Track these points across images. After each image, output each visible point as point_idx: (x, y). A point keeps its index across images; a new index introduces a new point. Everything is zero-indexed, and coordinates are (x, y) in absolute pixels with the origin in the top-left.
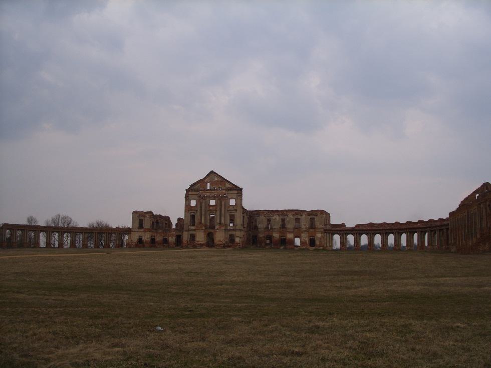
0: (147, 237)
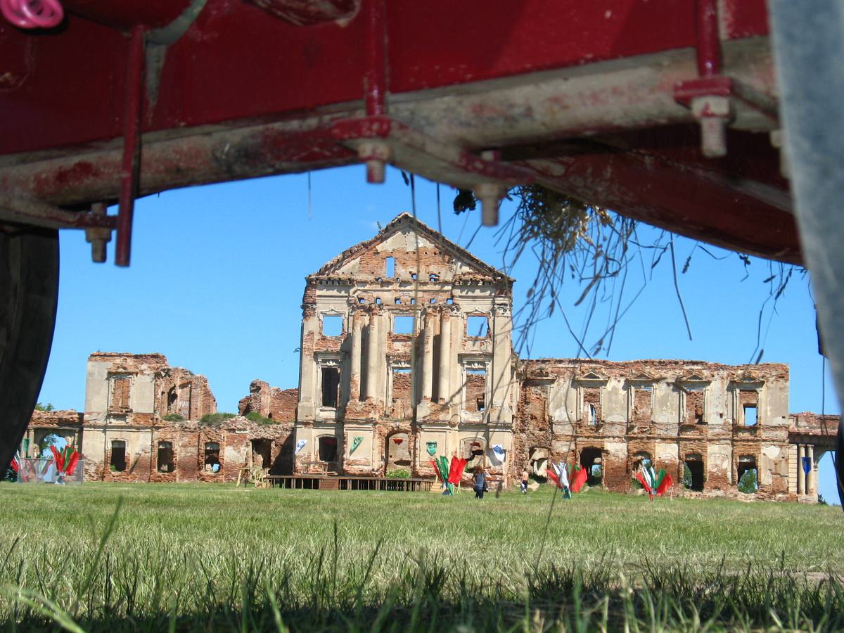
0: (139, 445)
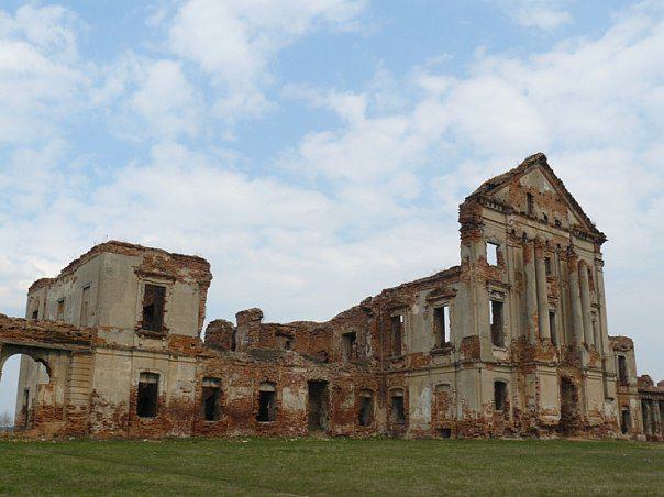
0: (180, 381)
